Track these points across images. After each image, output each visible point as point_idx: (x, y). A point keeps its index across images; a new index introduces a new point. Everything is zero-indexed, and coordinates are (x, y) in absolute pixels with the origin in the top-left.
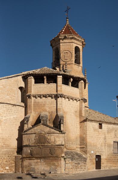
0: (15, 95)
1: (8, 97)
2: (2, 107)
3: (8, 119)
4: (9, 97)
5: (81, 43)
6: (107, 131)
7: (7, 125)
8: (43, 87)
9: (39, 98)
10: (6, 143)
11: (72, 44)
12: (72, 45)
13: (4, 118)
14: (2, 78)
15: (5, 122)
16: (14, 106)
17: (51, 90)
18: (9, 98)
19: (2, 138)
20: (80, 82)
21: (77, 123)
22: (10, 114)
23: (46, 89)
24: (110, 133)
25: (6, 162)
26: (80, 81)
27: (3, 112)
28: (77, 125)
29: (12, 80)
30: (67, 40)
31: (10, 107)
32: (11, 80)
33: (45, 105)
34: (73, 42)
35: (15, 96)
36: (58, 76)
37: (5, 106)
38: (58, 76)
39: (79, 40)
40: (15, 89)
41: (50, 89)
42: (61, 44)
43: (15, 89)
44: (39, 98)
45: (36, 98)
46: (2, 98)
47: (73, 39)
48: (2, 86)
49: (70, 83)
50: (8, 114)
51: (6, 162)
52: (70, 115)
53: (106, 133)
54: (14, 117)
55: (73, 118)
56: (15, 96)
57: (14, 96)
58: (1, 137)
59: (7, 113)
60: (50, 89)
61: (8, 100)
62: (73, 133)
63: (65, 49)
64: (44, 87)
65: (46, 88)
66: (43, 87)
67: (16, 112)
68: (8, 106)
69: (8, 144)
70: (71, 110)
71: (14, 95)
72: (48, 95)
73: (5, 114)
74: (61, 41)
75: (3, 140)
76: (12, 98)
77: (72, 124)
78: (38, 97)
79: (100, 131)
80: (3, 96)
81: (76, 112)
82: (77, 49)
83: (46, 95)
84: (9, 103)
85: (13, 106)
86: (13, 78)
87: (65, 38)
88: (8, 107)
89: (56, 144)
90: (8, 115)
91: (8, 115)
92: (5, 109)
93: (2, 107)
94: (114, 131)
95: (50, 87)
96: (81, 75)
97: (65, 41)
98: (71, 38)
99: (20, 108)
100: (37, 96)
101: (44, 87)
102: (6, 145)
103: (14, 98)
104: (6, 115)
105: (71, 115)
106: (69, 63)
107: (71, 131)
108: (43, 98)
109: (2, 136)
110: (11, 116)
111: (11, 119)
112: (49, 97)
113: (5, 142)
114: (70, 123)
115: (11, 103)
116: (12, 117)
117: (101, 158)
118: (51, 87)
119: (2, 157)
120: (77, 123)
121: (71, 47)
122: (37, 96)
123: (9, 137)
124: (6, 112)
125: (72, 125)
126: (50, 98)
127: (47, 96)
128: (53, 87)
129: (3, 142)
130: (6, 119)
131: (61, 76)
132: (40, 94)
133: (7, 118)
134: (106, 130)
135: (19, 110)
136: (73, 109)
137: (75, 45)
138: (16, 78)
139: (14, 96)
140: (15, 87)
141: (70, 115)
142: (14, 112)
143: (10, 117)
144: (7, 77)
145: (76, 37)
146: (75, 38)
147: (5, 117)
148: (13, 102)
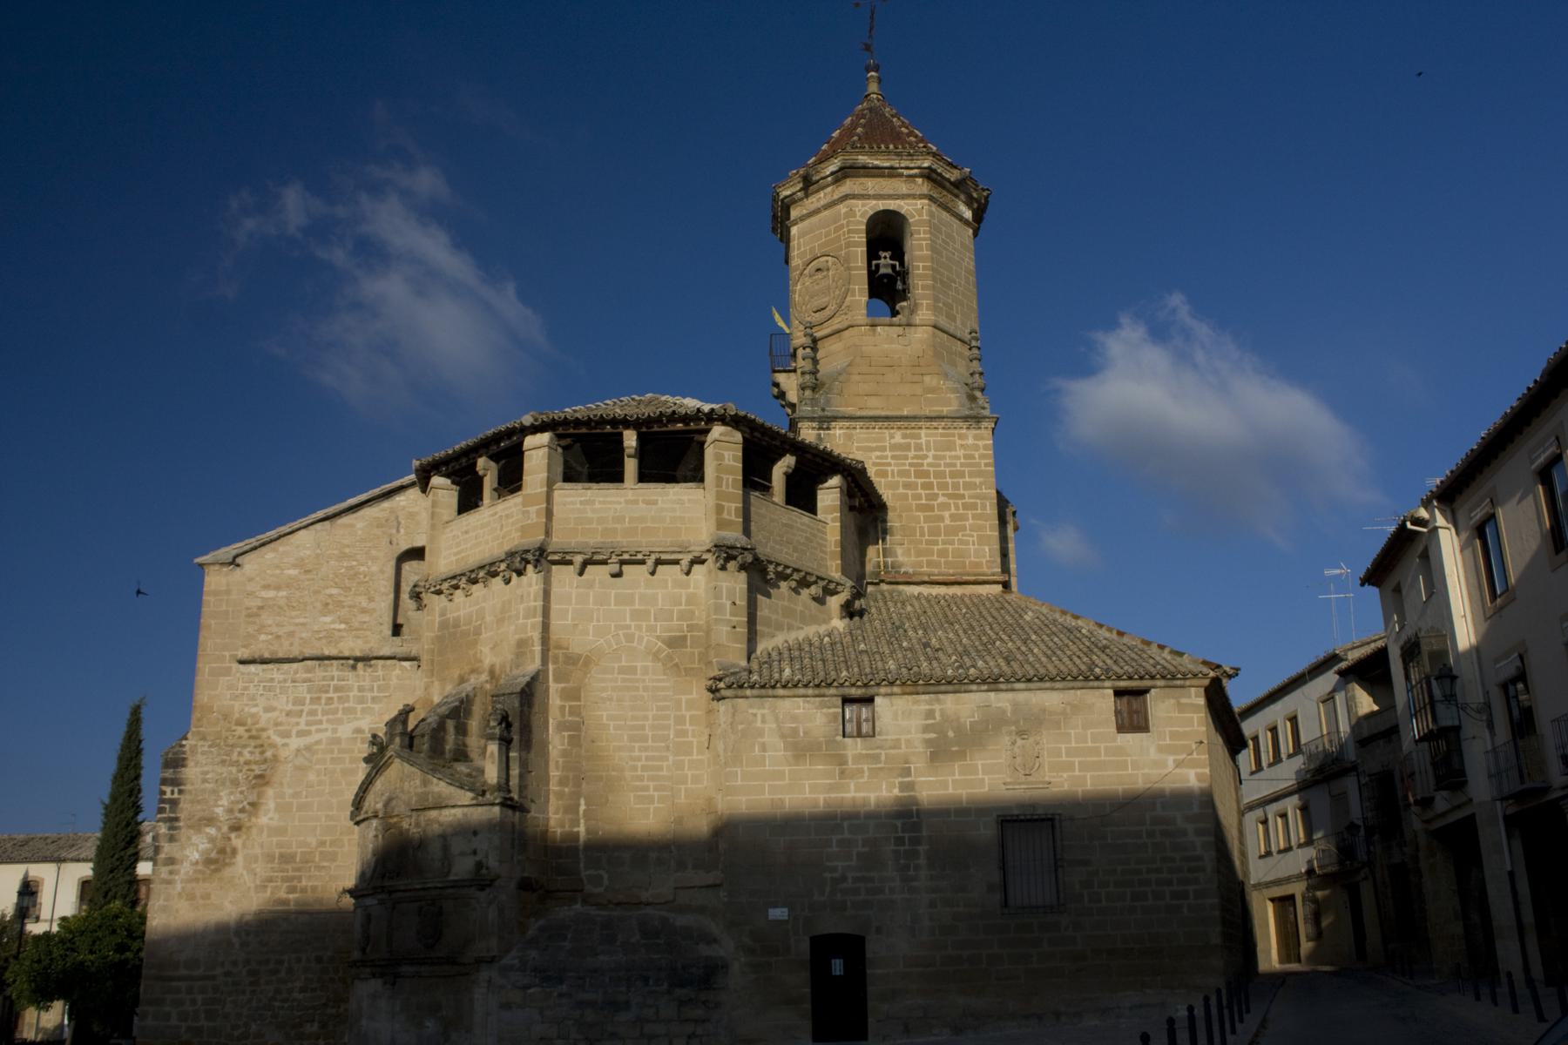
0: (371, 600)
1: (328, 619)
2: (285, 681)
3: (318, 742)
4: (333, 622)
5: (920, 180)
6: (928, 742)
7: (312, 777)
10: (304, 883)
11: (844, 210)
12: (851, 213)
13: (295, 743)
14: (296, 525)
15: (300, 761)
16: (360, 665)
18: (337, 626)
19: (282, 856)
20: (710, 437)
21: (680, 720)
22: (336, 711)
24: (962, 755)
25: (302, 990)
26: (707, 431)
27: (290, 707)
28: (683, 733)
29: (360, 525)
30: (822, 194)
31: (336, 673)
32: (352, 526)
33: (478, 632)
34: (845, 197)
35: (372, 605)
36: (529, 441)
37: (302, 675)
38: (529, 441)
39: (891, 168)
40: (374, 569)
42: (794, 230)
43: (374, 569)
46: (291, 634)
47: (845, 177)
48: (294, 566)
49: (631, 466)
50: (325, 713)
51: (302, 990)
52: (622, 671)
53: (918, 764)
54: (359, 731)
55: (646, 689)
56: (372, 605)
57: (364, 611)
58: (277, 851)
59: (312, 713)
61: (330, 637)
62: (646, 789)
63: (812, 249)
65: (500, 523)
67: (373, 699)
68: (319, 672)
69: (314, 888)
70: (630, 638)
71: (364, 604)
73: (303, 720)
74: (795, 213)
75: (289, 867)
76: (356, 625)
77: (643, 727)
79: (850, 753)
80: (302, 620)
81: (675, 642)
82: (886, 235)
84: (334, 652)
85: (354, 667)
86: (367, 512)
87: (808, 184)
88: (324, 679)
89: (452, 878)
90: (321, 722)
91: (321, 722)
92: (302, 690)
93: (285, 681)
94: (1006, 740)
96: (927, 379)
97: (814, 202)
98: (832, 173)
99: (397, 672)
102: (304, 890)
103: (366, 618)
104: (308, 724)
105: (633, 670)
106: (836, 324)
107: (628, 774)
109: (280, 845)
110: (339, 722)
111: (337, 741)
113: (299, 879)
114: (617, 728)
115: (347, 654)
116: (345, 731)
117: (869, 955)
118: (507, 516)
119: (280, 962)
120: (680, 720)
121: (842, 226)
122: (446, 585)
123: (323, 843)
124: (306, 708)
125: (632, 739)
129: (284, 880)
130: (308, 748)
131: (545, 438)
133: (315, 737)
134: (917, 737)
135: (394, 681)
136: (651, 629)
137: (865, 210)
138: (386, 504)
139: (364, 611)
140: (374, 559)
141: (622, 671)
142: (361, 700)
143: (334, 731)
144: (320, 514)
145: (863, 159)
146: (864, 167)
147: (301, 734)
148: (360, 642)
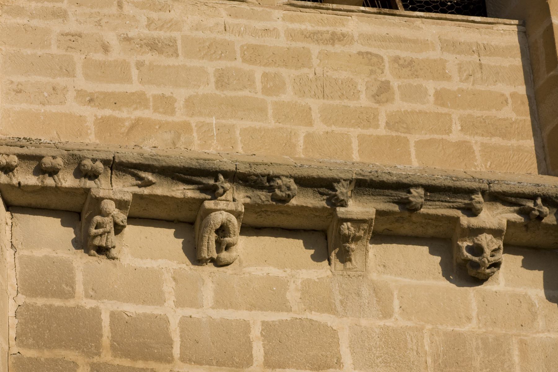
8: (212, 49)
9: (166, 239)
17: (397, 122)
23: (288, 96)
41: (382, 92)
44: (150, 250)
45: (84, 243)
60: (382, 92)
64: (254, 54)
66: (212, 49)
72: (365, 186)
78: (144, 213)
83: (322, 185)
95: (372, 61)
100: (115, 190)
101: (254, 54)
108: (243, 246)
112: (384, 233)
118: (408, 67)
122: (124, 188)
126: (412, 268)
127: (358, 208)
128: (438, 71)
132: (197, 148)
